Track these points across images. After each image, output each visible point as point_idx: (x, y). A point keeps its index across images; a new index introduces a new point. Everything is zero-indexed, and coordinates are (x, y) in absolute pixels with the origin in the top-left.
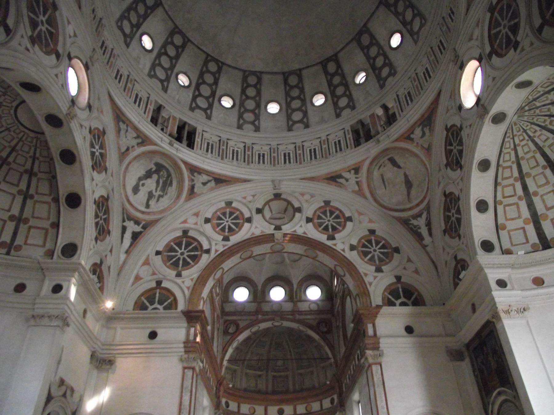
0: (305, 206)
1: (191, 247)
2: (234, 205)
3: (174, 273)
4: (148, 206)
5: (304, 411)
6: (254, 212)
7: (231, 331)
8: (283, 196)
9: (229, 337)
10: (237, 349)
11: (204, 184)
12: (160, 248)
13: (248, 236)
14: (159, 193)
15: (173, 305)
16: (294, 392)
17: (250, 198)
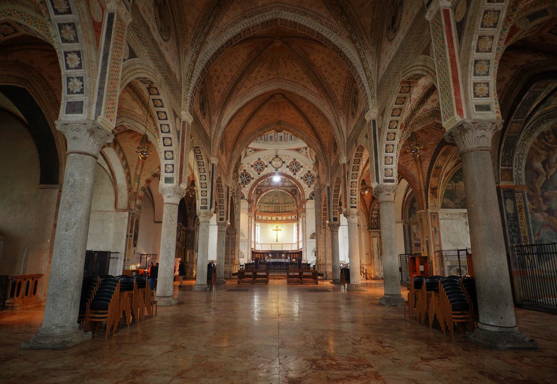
0: (286, 161)
6: (268, 163)
7: (259, 193)
8: (279, 156)
9: (258, 195)
10: (261, 199)
11: (250, 152)
13: (266, 173)
15: (243, 198)
16: (282, 212)
17: (267, 157)
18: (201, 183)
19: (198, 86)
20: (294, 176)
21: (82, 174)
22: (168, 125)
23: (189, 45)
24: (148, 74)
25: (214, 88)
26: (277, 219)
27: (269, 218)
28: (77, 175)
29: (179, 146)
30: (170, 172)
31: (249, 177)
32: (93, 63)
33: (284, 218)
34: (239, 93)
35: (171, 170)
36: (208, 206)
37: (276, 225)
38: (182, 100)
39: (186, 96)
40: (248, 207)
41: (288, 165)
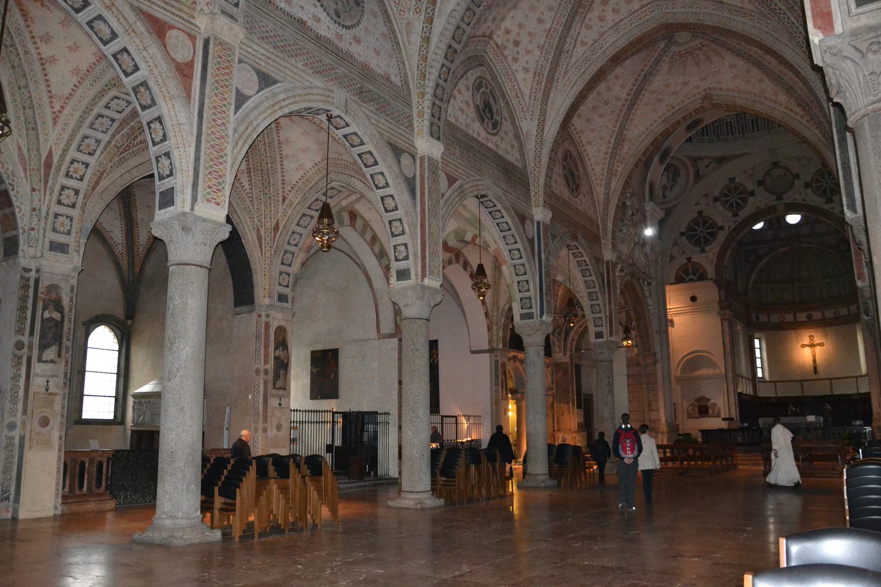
1: (707, 226)
2: (737, 181)
3: (699, 249)
4: (664, 197)
5: (832, 316)
8: (781, 164)
11: (707, 166)
12: (683, 230)
14: (671, 183)
18: (515, 266)
19: (446, 81)
20: (827, 207)
21: (182, 295)
22: (382, 174)
23: (411, 12)
24: (310, 101)
25: (514, 67)
26: (809, 317)
27: (789, 318)
28: (177, 298)
29: (415, 206)
30: (403, 259)
31: (714, 225)
32: (181, 126)
33: (829, 314)
34: (573, 60)
35: (404, 254)
36: (536, 310)
37: (812, 332)
38: (415, 116)
39: (420, 108)
40: (718, 298)
41: (808, 180)
